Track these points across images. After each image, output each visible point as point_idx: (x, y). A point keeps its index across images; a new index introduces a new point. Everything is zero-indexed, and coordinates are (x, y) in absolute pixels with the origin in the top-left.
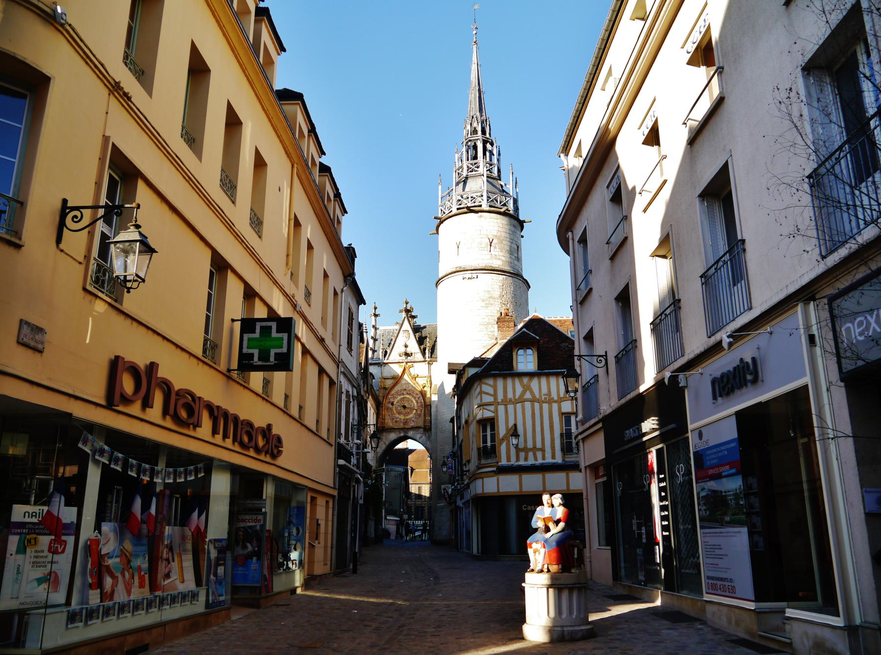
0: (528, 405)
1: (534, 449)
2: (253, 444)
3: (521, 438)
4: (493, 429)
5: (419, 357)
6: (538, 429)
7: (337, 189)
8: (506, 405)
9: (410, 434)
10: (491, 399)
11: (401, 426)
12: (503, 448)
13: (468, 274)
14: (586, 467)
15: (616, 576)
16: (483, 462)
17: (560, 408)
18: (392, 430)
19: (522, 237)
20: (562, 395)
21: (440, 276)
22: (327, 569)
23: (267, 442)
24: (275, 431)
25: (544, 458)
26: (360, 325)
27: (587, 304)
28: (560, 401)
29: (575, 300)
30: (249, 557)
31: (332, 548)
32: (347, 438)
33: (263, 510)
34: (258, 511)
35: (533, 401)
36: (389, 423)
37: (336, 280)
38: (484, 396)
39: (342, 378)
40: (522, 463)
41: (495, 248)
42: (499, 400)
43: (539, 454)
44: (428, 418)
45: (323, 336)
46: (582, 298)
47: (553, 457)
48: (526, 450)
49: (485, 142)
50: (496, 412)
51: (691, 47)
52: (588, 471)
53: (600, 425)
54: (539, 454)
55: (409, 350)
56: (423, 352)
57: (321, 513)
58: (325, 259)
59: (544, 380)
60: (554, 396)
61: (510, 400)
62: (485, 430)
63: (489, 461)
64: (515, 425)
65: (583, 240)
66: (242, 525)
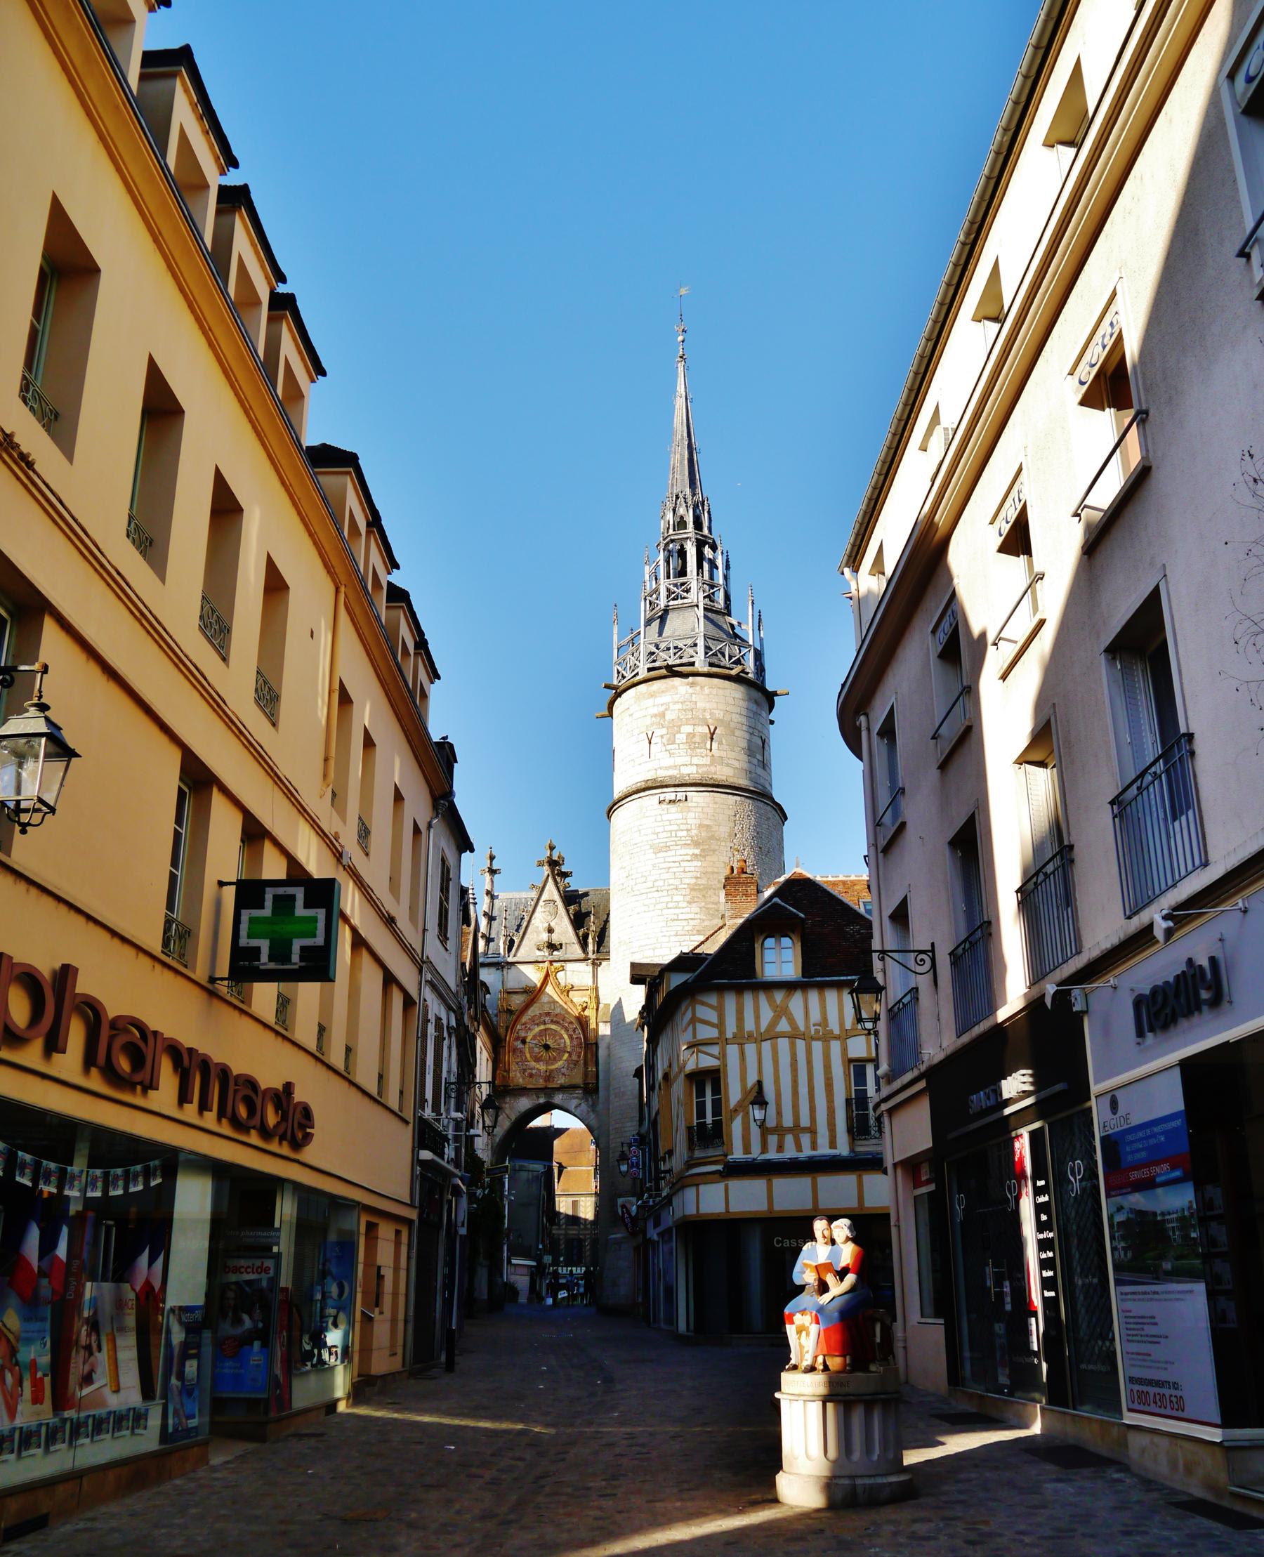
0: (783, 1044)
1: (796, 1129)
2: (256, 1121)
3: (772, 1108)
4: (717, 1090)
5: (577, 951)
6: (803, 1090)
7: (421, 633)
8: (741, 1045)
9: (558, 1098)
10: (712, 1033)
11: (541, 1083)
12: (737, 1127)
13: (669, 794)
14: (895, 1165)
15: (954, 1376)
16: (698, 1154)
17: (844, 1050)
18: (523, 1091)
19: (772, 722)
20: (848, 1025)
21: (616, 796)
22: (396, 1364)
23: (284, 1118)
24: (298, 1096)
25: (814, 1146)
26: (464, 892)
27: (896, 851)
28: (845, 1036)
29: (873, 844)
30: (247, 1340)
31: (406, 1321)
32: (436, 1108)
33: (275, 1249)
34: (264, 1250)
35: (793, 1036)
36: (517, 1078)
37: (418, 806)
38: (699, 1026)
39: (428, 994)
40: (772, 1155)
41: (720, 743)
42: (729, 1035)
43: (805, 1139)
44: (592, 1069)
45: (393, 913)
46: (886, 840)
47: (833, 1144)
48: (780, 1130)
49: (700, 544)
50: (723, 1056)
51: (1088, 373)
52: (899, 1172)
53: (922, 1085)
54: (805, 1139)
55: (555, 938)
56: (584, 944)
57: (385, 1254)
58: (397, 766)
59: (813, 996)
60: (834, 1027)
61: (750, 1036)
62: (701, 1093)
63: (710, 1152)
64: (760, 1083)
65: (888, 731)
66: (233, 1278)
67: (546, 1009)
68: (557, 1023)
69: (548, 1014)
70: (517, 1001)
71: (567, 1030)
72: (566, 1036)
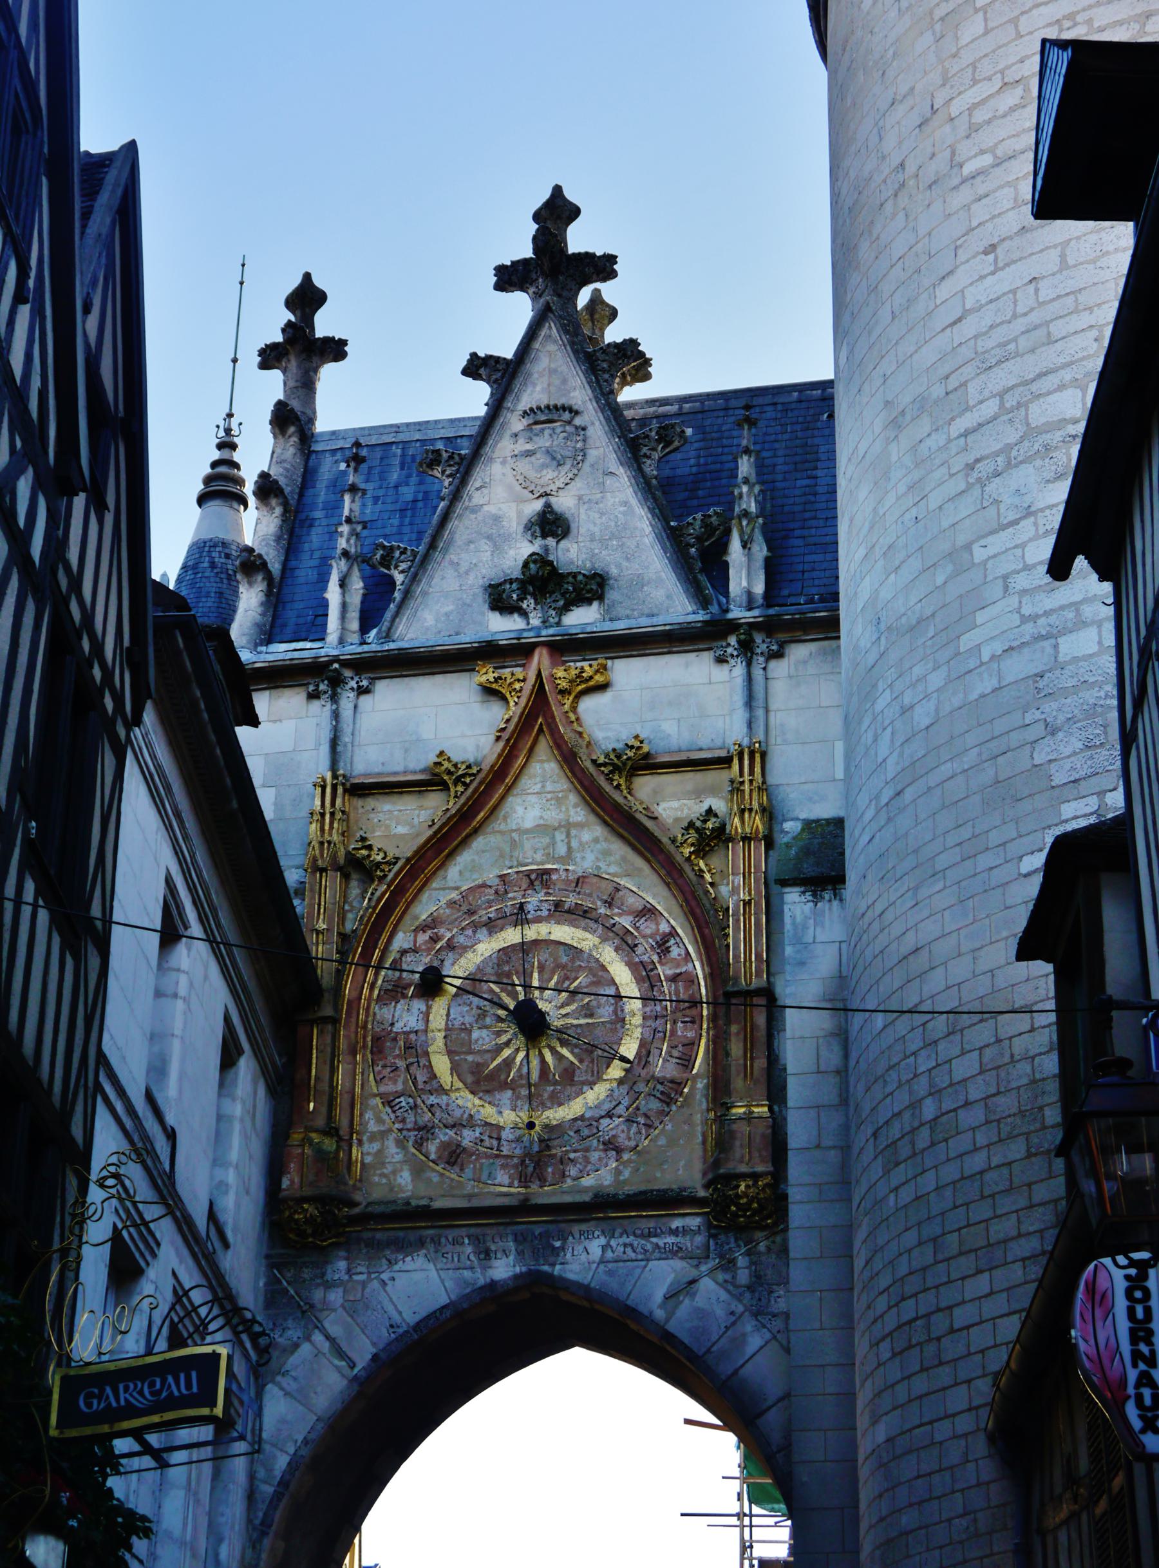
9: (585, 1258)
11: (503, 1185)
18: (411, 1225)
36: (389, 1166)
56: (702, 565)
67: (533, 857)
68: (579, 915)
69: (540, 878)
70: (398, 826)
71: (626, 944)
72: (622, 975)
